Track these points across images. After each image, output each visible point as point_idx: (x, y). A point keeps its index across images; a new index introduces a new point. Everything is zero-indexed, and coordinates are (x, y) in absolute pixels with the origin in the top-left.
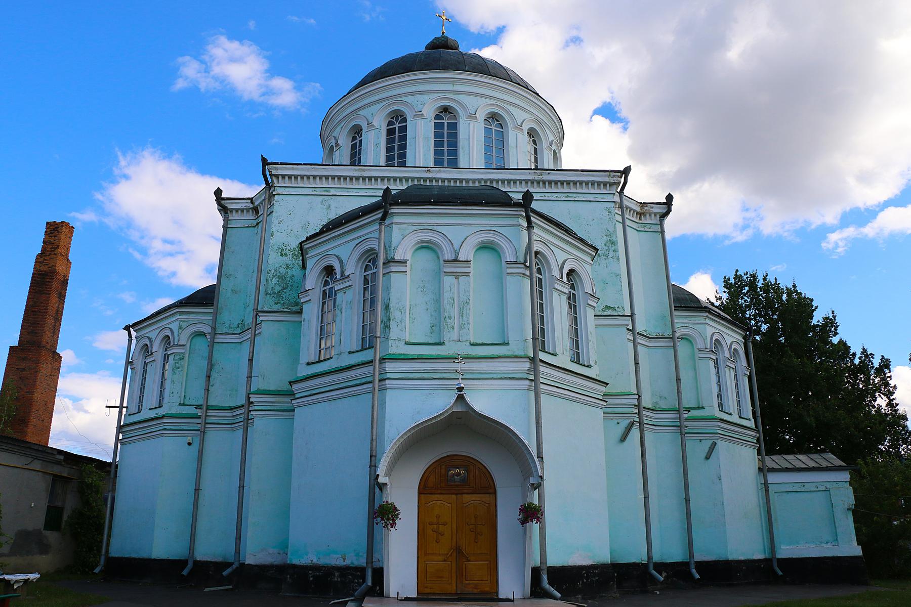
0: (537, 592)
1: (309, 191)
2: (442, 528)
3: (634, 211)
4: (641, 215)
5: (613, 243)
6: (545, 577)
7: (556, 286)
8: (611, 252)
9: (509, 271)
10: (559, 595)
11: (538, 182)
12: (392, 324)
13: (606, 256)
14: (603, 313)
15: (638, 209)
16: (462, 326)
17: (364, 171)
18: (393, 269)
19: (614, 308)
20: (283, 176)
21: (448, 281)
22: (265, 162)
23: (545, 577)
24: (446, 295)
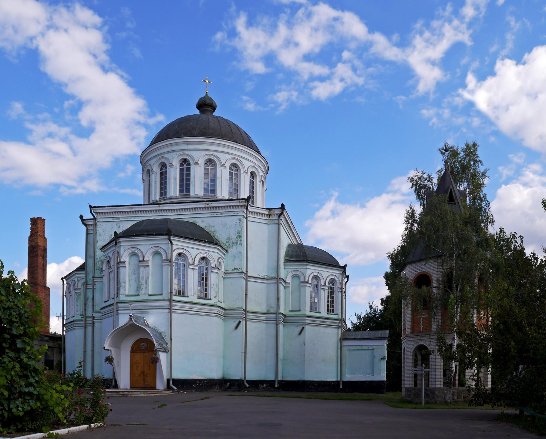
0: (168, 387)
1: (111, 220)
2: (138, 365)
3: (265, 214)
4: (269, 215)
5: (240, 237)
6: (171, 382)
7: (190, 267)
8: (239, 242)
9: (164, 264)
10: (176, 388)
11: (208, 208)
12: (121, 288)
13: (236, 243)
14: (232, 272)
15: (267, 213)
16: (146, 288)
17: (132, 208)
18: (121, 265)
19: (237, 269)
20: (100, 213)
21: (142, 269)
22: (91, 207)
23: (171, 382)
24: (141, 275)
